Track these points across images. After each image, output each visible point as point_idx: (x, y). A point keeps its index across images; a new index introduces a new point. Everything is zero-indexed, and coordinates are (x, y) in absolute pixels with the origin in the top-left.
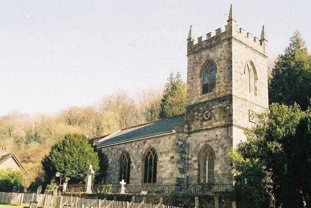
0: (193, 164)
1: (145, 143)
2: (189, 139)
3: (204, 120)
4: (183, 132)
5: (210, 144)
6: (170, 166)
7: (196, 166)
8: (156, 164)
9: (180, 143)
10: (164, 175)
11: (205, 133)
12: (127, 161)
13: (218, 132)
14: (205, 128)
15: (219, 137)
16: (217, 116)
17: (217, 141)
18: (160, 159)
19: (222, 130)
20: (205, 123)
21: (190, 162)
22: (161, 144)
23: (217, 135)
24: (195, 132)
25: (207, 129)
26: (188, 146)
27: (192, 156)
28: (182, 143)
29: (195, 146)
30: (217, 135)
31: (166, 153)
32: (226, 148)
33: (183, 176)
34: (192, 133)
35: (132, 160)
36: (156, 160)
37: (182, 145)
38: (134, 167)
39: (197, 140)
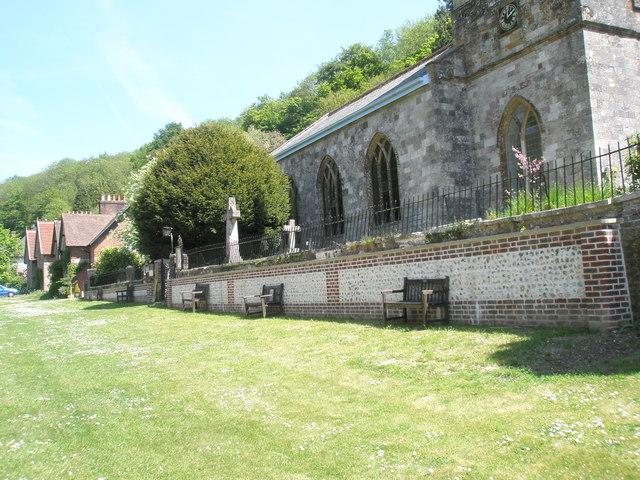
0: (489, 155)
1: (365, 126)
2: (471, 93)
3: (503, 33)
4: (450, 78)
5: (525, 93)
6: (427, 172)
7: (496, 161)
8: (395, 173)
9: (445, 107)
10: (416, 197)
11: (511, 67)
12: (334, 178)
13: (543, 56)
14: (509, 52)
15: (548, 68)
16: (535, 10)
17: (543, 83)
18: (402, 159)
19: (554, 46)
20: (506, 41)
21: (479, 153)
22: (400, 121)
23: (540, 66)
24: (483, 70)
25: (515, 56)
26: (468, 113)
27: (483, 137)
28: (452, 108)
29: (486, 108)
30: (540, 66)
31: (417, 140)
32: (571, 93)
33: (466, 194)
34: (475, 75)
35: (343, 175)
36: (394, 163)
37: (452, 114)
38: (351, 192)
39: (496, 86)
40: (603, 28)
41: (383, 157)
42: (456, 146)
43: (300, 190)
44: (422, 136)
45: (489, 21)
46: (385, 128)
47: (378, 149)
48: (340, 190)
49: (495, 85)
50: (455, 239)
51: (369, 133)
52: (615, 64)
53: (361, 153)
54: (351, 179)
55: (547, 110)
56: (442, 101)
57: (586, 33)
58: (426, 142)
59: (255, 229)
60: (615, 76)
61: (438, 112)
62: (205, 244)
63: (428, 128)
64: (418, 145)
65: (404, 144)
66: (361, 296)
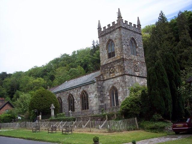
0: (108, 97)
1: (81, 88)
2: (104, 83)
3: (111, 73)
4: (100, 80)
5: (115, 85)
6: (95, 99)
7: (109, 98)
8: (87, 99)
9: (99, 86)
10: (92, 105)
11: (112, 80)
12: (72, 99)
13: (118, 79)
14: (112, 77)
15: (119, 81)
16: (117, 70)
17: (118, 84)
18: (89, 96)
19: (120, 77)
20: (111, 74)
21: (106, 96)
22: (89, 88)
23: (118, 81)
24: (107, 80)
25: (113, 78)
26: (103, 87)
27: (106, 93)
28: (100, 87)
29: (107, 87)
30: (118, 81)
31: (93, 93)
32: (123, 87)
33: (103, 104)
34: (105, 80)
35: (75, 98)
36: (87, 97)
37: (100, 88)
38: (76, 102)
39: (108, 84)
40: (129, 75)
41: (85, 95)
42: (101, 94)
43: (63, 101)
44: (94, 92)
45: (108, 70)
46: (85, 89)
47: (83, 93)
48: (74, 102)
49: (109, 83)
50: (160, 120)
51: (81, 90)
52: (131, 82)
53: (79, 94)
54: (76, 99)
55: (119, 89)
56: (98, 85)
57: (126, 76)
58: (95, 93)
59: (58, 110)
60: (131, 84)
61: (98, 87)
62: (46, 114)
63: (95, 90)
64: (93, 94)
65: (90, 93)
66: (181, 137)
